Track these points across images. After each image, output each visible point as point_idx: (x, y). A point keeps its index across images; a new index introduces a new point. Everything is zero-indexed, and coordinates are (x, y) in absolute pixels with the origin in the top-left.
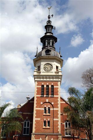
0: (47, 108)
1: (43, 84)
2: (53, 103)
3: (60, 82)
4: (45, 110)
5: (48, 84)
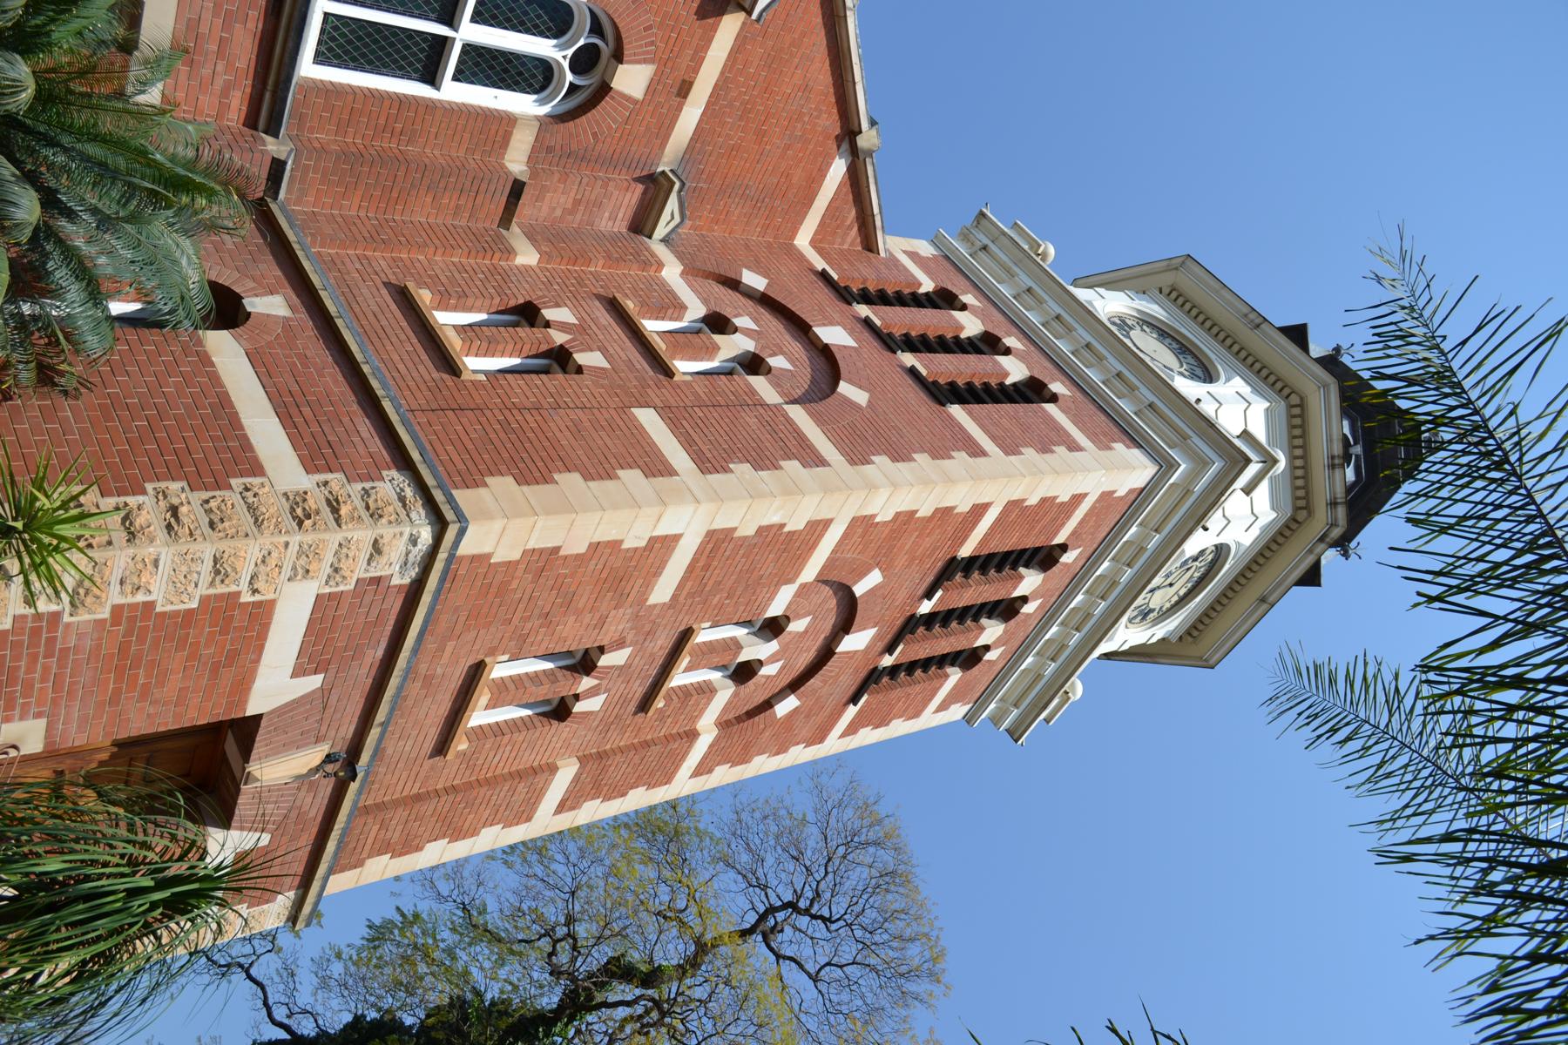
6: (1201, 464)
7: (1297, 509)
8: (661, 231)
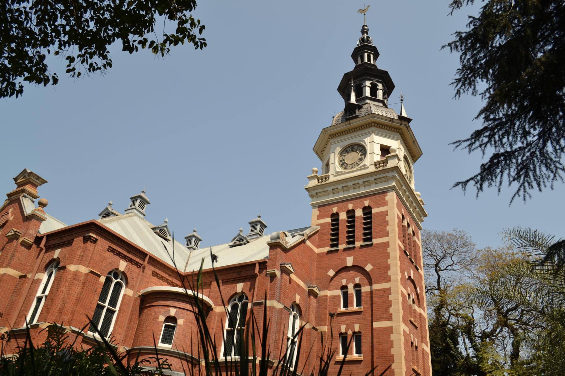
0: (351, 286)
1: (335, 210)
2: (368, 268)
3: (394, 193)
4: (346, 295)
5: (350, 208)
6: (394, 178)
7: (398, 132)
8: (317, 292)
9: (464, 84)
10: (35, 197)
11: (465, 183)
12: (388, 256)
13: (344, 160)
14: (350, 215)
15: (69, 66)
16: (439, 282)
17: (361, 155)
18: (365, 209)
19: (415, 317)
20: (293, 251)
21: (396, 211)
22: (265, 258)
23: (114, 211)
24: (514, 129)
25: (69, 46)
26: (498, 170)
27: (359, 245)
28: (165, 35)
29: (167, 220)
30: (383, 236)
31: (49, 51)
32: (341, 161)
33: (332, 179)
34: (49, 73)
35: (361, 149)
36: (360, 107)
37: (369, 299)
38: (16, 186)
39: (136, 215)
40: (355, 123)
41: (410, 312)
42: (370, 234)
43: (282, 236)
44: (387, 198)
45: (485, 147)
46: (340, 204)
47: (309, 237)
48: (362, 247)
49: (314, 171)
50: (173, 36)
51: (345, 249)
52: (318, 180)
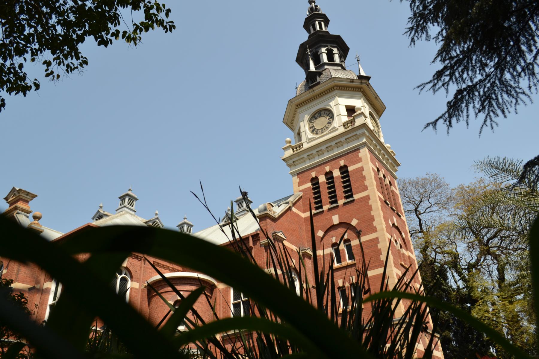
1: (313, 174)
2: (354, 222)
3: (366, 149)
4: (337, 251)
6: (363, 134)
7: (360, 91)
9: (416, 31)
10: (29, 212)
11: (435, 123)
12: (370, 208)
13: (313, 126)
14: (329, 176)
15: (47, 70)
16: (421, 225)
17: (329, 119)
18: (341, 168)
19: (405, 260)
20: (281, 219)
21: (371, 165)
22: (256, 231)
23: (106, 213)
24: (472, 63)
25: (41, 53)
26: (463, 105)
27: (342, 203)
28: (134, 25)
29: (157, 212)
30: (363, 191)
31: (25, 59)
32: (311, 128)
33: (306, 146)
34: (29, 81)
35: (328, 113)
36: (320, 74)
37: (360, 251)
38: (8, 205)
39: (127, 212)
40: (318, 89)
41: (400, 256)
42: (351, 190)
43: (269, 207)
44: (360, 155)
45: (447, 86)
46: (318, 168)
47: (294, 204)
48: (345, 204)
49: (287, 142)
50: (142, 24)
51: (330, 209)
52: (293, 150)
